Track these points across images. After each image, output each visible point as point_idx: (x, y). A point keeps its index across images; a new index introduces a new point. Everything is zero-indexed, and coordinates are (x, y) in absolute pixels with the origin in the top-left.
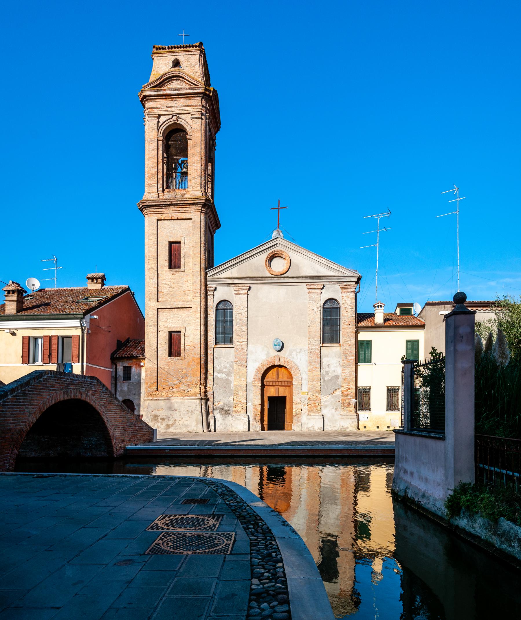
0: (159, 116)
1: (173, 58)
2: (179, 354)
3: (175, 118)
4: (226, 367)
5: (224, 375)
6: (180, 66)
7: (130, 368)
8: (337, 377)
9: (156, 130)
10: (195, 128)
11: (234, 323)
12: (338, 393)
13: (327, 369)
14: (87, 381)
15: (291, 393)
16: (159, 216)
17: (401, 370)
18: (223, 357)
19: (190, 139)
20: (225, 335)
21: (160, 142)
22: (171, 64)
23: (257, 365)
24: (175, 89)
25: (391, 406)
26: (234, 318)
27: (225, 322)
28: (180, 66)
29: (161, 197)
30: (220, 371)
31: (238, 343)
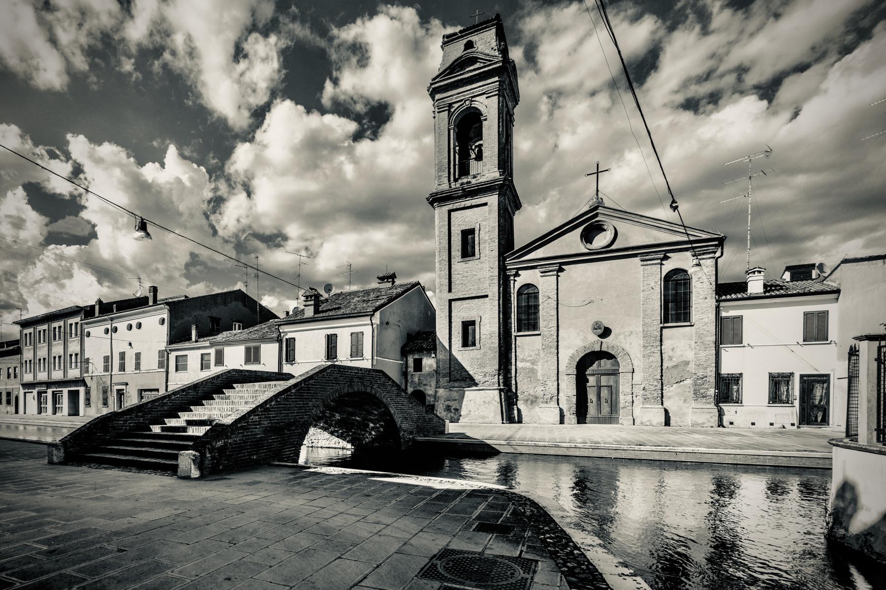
0: (450, 105)
1: (465, 41)
3: (467, 102)
6: (473, 47)
7: (420, 360)
9: (447, 120)
10: (489, 107)
11: (541, 307)
12: (689, 382)
14: (376, 374)
15: (617, 382)
19: (486, 120)
20: (529, 321)
21: (452, 131)
22: (463, 48)
23: (571, 352)
24: (468, 72)
25: (775, 398)
26: (541, 301)
27: (529, 307)
28: (473, 47)
29: (453, 187)
30: (523, 360)
31: (545, 329)
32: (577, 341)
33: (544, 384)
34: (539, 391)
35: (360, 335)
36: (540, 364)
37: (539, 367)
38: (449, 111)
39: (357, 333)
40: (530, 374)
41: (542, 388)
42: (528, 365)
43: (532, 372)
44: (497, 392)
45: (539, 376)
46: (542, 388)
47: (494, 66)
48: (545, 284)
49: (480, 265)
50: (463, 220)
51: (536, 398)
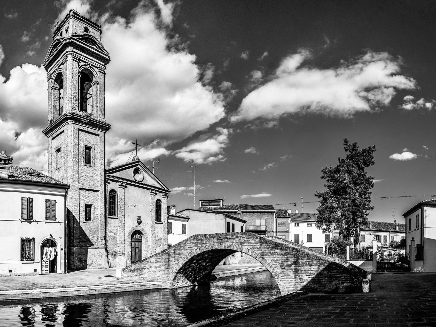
2: (90, 219)
4: (114, 230)
5: (113, 234)
8: (161, 239)
13: (157, 234)
16: (80, 127)
17: (197, 234)
18: (113, 223)
30: (111, 232)
32: (130, 225)
33: (120, 246)
34: (117, 249)
35: (53, 202)
36: (118, 234)
37: (117, 237)
38: (79, 65)
39: (51, 201)
40: (114, 240)
41: (119, 248)
42: (113, 234)
43: (115, 238)
44: (104, 249)
45: (118, 242)
46: (119, 248)
47: (102, 55)
48: (120, 192)
49: (94, 171)
50: (87, 139)
51: (116, 253)
